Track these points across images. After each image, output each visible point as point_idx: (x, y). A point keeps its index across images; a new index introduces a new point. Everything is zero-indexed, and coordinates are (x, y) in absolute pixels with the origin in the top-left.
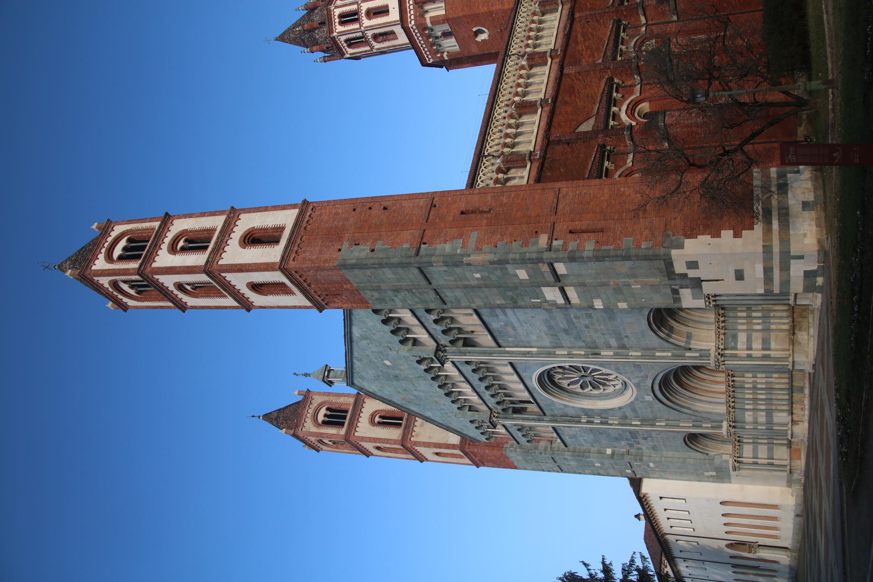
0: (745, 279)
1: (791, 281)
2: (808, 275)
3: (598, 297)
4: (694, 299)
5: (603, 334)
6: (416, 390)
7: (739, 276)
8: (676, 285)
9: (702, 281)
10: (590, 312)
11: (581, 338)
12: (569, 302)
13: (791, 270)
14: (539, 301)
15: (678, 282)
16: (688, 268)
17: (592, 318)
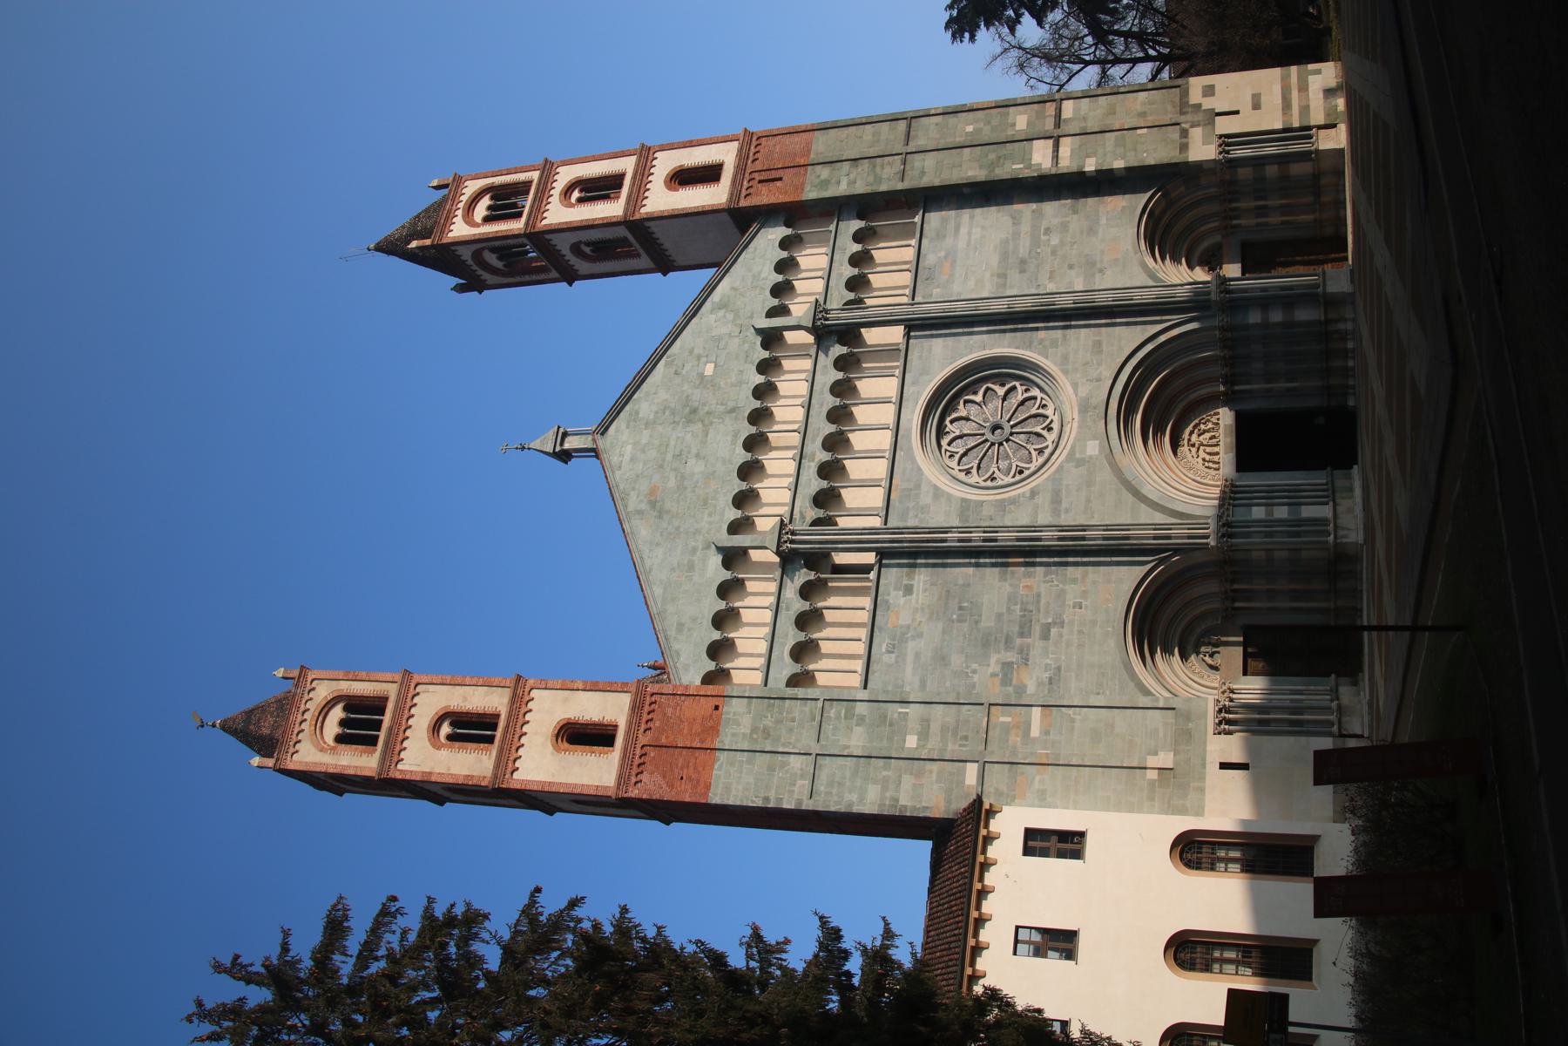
0: (1263, 106)
1: (1311, 107)
2: (1329, 93)
3: (1094, 154)
4: (1203, 144)
5: (1071, 267)
6: (697, 456)
7: (1256, 106)
8: (1186, 122)
9: (1219, 114)
10: (1067, 219)
11: (1036, 279)
12: (1057, 163)
13: (1310, 89)
14: (1021, 166)
15: (1189, 117)
16: (1205, 95)
17: (1067, 231)
